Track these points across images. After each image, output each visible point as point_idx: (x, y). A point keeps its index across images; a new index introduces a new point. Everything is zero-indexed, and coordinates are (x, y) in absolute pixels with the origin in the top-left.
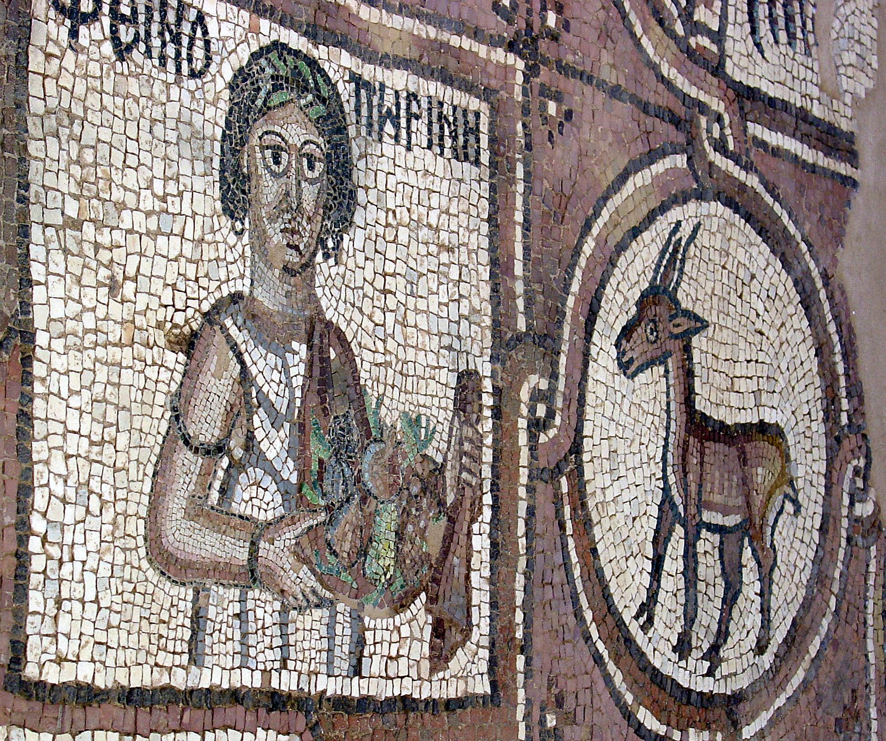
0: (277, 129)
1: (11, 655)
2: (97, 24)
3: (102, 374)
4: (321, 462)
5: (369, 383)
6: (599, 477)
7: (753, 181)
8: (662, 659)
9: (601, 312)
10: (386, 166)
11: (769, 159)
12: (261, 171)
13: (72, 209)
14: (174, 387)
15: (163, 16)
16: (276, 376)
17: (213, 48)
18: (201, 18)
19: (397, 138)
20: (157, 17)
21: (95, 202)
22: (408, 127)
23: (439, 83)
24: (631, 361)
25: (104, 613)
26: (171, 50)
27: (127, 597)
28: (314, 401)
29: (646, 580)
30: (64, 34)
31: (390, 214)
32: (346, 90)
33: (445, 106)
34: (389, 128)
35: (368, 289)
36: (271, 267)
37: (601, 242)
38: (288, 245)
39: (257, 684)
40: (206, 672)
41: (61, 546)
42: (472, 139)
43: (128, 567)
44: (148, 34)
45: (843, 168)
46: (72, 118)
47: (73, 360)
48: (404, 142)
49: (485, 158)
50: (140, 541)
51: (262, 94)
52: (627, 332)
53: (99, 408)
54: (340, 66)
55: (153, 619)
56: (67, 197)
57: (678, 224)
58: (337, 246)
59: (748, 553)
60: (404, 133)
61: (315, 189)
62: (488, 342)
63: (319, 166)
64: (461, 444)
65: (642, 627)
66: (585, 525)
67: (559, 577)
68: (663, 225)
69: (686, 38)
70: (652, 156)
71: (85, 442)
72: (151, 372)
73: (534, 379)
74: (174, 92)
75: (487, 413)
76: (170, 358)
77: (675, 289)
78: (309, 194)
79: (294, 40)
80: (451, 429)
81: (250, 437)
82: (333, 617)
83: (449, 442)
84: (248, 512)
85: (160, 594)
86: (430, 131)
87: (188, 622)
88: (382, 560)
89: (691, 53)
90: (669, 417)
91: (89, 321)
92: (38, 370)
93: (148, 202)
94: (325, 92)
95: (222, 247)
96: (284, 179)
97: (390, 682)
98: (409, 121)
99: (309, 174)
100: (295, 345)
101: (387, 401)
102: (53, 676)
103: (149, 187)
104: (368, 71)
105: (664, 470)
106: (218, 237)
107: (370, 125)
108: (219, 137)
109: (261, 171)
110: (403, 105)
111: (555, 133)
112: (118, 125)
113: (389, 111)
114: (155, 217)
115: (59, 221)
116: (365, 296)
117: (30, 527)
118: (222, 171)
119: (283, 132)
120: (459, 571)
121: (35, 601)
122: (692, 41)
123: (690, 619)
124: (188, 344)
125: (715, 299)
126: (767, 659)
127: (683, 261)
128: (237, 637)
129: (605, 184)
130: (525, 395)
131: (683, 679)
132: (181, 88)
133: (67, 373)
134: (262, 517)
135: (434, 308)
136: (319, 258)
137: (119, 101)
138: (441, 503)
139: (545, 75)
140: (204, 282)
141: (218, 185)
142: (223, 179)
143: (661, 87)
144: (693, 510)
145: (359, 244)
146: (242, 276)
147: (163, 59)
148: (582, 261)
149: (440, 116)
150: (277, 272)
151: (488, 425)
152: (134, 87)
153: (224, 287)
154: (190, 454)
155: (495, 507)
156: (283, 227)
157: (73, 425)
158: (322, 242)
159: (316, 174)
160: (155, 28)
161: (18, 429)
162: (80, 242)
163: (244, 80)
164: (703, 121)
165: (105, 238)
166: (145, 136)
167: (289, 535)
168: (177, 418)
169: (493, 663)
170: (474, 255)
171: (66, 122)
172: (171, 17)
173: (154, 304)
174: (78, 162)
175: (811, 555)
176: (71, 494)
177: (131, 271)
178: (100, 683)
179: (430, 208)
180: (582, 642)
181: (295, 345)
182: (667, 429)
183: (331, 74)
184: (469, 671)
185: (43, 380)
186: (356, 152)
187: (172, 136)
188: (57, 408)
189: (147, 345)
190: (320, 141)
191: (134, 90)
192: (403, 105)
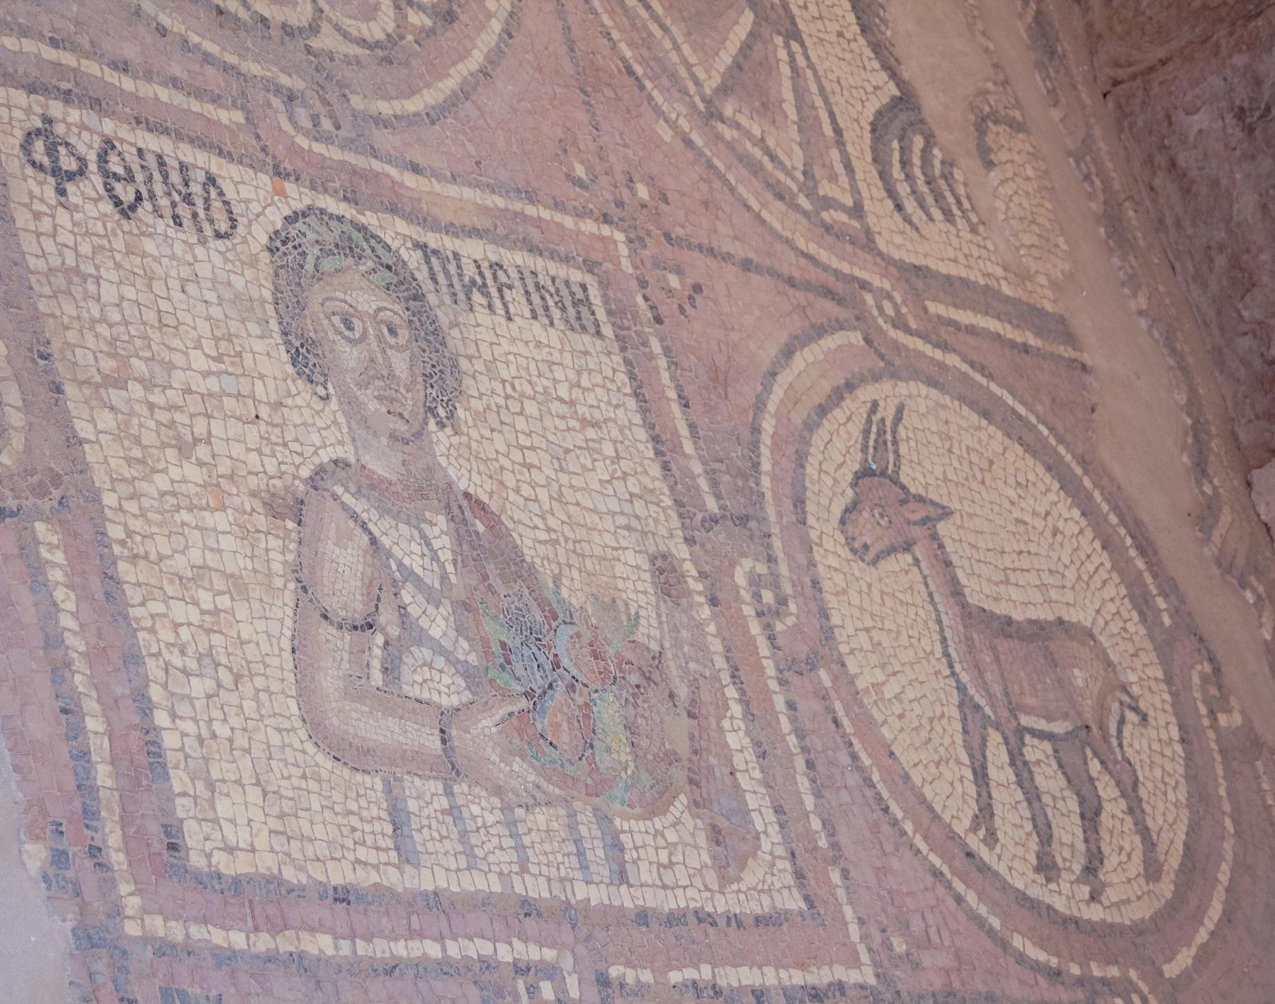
0: (341, 296)
4: (503, 645)
5: (537, 561)
7: (953, 360)
8: (1023, 878)
12: (331, 336)
15: (166, 177)
18: (211, 180)
19: (490, 307)
23: (525, 254)
27: (295, 781)
29: (972, 790)
30: (50, 193)
31: (507, 385)
32: (413, 259)
33: (540, 276)
34: (477, 297)
38: (389, 412)
40: (426, 873)
42: (584, 311)
45: (1067, 352)
46: (85, 278)
54: (397, 234)
56: (99, 355)
58: (451, 416)
59: (1095, 766)
65: (984, 841)
66: (867, 725)
67: (853, 779)
70: (820, 331)
73: (747, 564)
77: (896, 472)
78: (400, 364)
80: (659, 615)
87: (384, 815)
88: (616, 753)
89: (828, 228)
94: (387, 259)
96: (363, 345)
97: (669, 892)
103: (198, 346)
108: (270, 299)
109: (331, 336)
111: (687, 307)
113: (473, 282)
117: (150, 700)
119: (347, 298)
120: (721, 771)
122: (824, 215)
123: (1044, 833)
126: (1166, 888)
130: (740, 578)
131: (1060, 904)
132: (208, 249)
136: (432, 425)
140: (295, 446)
143: (803, 261)
150: (384, 441)
153: (321, 452)
155: (745, 702)
156: (376, 393)
161: (107, 593)
164: (869, 299)
167: (487, 723)
170: (627, 432)
172: (175, 177)
175: (1181, 770)
182: (939, 622)
185: (122, 543)
190: (397, 307)
192: (488, 274)
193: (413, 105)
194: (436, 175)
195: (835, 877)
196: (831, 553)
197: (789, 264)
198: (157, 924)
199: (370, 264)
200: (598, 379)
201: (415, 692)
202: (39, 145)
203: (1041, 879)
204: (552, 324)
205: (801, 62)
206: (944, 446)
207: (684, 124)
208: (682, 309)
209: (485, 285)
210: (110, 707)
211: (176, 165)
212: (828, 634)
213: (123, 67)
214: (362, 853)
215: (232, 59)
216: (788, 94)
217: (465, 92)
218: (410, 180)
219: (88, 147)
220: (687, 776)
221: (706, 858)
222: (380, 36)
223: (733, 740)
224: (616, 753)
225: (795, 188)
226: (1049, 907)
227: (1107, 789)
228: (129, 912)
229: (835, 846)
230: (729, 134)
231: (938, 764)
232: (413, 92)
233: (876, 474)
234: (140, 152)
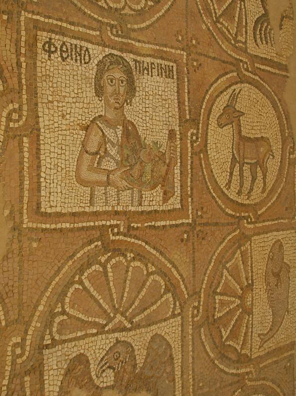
0: (112, 74)
1: (37, 206)
2: (56, 54)
3: (60, 137)
5: (142, 134)
6: (213, 153)
7: (257, 78)
9: (212, 113)
10: (145, 81)
11: (262, 73)
13: (50, 98)
14: (82, 139)
15: (76, 50)
16: (113, 135)
17: (91, 56)
18: (87, 49)
20: (74, 50)
21: (57, 96)
22: (152, 71)
24: (222, 124)
25: (64, 195)
26: (78, 58)
28: (125, 140)
29: (228, 177)
30: (47, 57)
34: (146, 72)
35: (141, 112)
36: (111, 108)
39: (110, 209)
40: (95, 207)
41: (50, 180)
42: (171, 73)
43: (70, 184)
44: (71, 54)
45: (284, 73)
47: (52, 135)
48: (150, 75)
49: (175, 77)
50: (74, 177)
51: (107, 66)
53: (60, 146)
55: (78, 195)
57: (235, 89)
58: (131, 101)
59: (259, 169)
60: (150, 73)
61: (124, 88)
62: (178, 122)
63: (125, 83)
64: (170, 147)
65: (227, 189)
66: (208, 165)
68: (230, 91)
69: (235, 44)
71: (57, 154)
72: (76, 136)
73: (192, 130)
74: (80, 68)
75: (178, 139)
76: (81, 132)
78: (122, 90)
81: (106, 149)
82: (133, 192)
83: (167, 147)
84: (106, 168)
85: (80, 190)
86: (158, 72)
87: (89, 196)
90: (234, 137)
91: (56, 125)
92: (41, 138)
93: (73, 95)
94: (126, 64)
95: (96, 104)
98: (152, 70)
99: (122, 85)
100: (118, 127)
101: (147, 139)
102: (49, 211)
104: (139, 58)
105: (232, 150)
106: (95, 102)
107: (140, 71)
110: (150, 66)
111: (196, 70)
112: (63, 77)
113: (146, 68)
114: (75, 99)
115: (47, 101)
116: (139, 113)
118: (95, 85)
121: (43, 193)
122: (237, 45)
123: (241, 186)
124: (86, 128)
125: (247, 108)
126: (265, 195)
127: (237, 99)
128: (104, 198)
129: (212, 82)
131: (240, 201)
133: (50, 138)
134: (110, 169)
135: (161, 115)
136: (125, 105)
137: (64, 71)
138: (165, 162)
139: (193, 55)
140: (90, 113)
141: (94, 89)
142: (95, 88)
143: (228, 56)
144: (242, 160)
145: (137, 101)
146: (102, 111)
147: (76, 60)
148: (206, 101)
149: (161, 68)
151: (179, 142)
152: (68, 67)
154: (88, 155)
155: (181, 162)
157: (52, 150)
158: (126, 101)
159: (124, 84)
160: (73, 53)
161: (36, 153)
162: (53, 106)
163: (101, 63)
164: (241, 64)
165: (60, 105)
166: (71, 79)
167: (119, 173)
168: (84, 147)
169: (181, 200)
171: (48, 77)
172: (78, 50)
173: (76, 119)
174: (52, 87)
175: (278, 168)
176: (52, 167)
177: (68, 112)
178: (63, 212)
179: (159, 90)
180: (208, 194)
181: (118, 127)
182: (233, 140)
183: (127, 60)
184: (175, 203)
185: (43, 140)
186: (136, 78)
187: (80, 78)
189: (74, 130)
191: (68, 68)
192: (150, 66)
194: (144, 42)
195: (190, 200)
197: (225, 58)
199: (121, 66)
200: (170, 89)
201: (104, 167)
202: (47, 45)
203: (237, 196)
204: (162, 77)
205: (243, 7)
207: (209, 24)
208: (195, 70)
209: (149, 69)
210: (30, 179)
211: (79, 47)
212: (206, 146)
214: (81, 205)
215: (100, 19)
216: (237, 15)
218: (137, 44)
221: (161, 198)
222: (140, 8)
223: (176, 171)
225: (232, 38)
226: (237, 202)
228: (25, 222)
229: (191, 193)
230: (219, 26)
231: (222, 173)
232: (144, 22)
233: (229, 107)
234: (71, 45)
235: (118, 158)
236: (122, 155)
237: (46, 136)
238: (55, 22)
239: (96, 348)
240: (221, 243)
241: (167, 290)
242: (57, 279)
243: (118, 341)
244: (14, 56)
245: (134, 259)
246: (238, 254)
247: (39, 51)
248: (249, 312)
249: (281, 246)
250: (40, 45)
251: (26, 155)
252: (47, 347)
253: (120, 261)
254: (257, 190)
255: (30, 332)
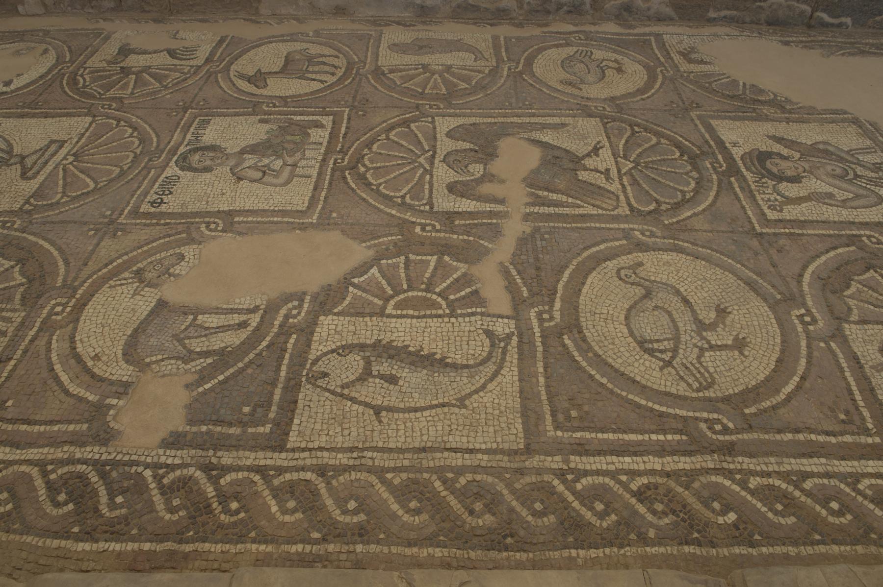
7: (227, 59)
8: (335, 79)
13: (204, 203)
32: (189, 147)
37: (235, 92)
45: (229, 38)
52: (256, 86)
66: (300, 96)
68: (234, 79)
70: (217, 81)
78: (211, 154)
79: (175, 158)
88: (297, 138)
89: (194, 73)
102: (306, 205)
104: (185, 143)
123: (327, 72)
124: (240, 179)
126: (341, 56)
130: (266, 109)
131: (341, 74)
152: (179, 191)
184: (327, 121)
188: (248, 205)
193: (155, 140)
194: (171, 139)
196: (265, 92)
198: (315, 217)
206: (247, 65)
210: (273, 216)
213: (139, 187)
217: (154, 130)
218: (172, 144)
219: (155, 197)
220: (304, 129)
224: (297, 138)
227: (321, 59)
232: (152, 139)
233: (249, 80)
235: (272, 158)
236: (272, 155)
237: (237, 206)
238: (134, 199)
239: (443, 174)
240: (376, 88)
241: (409, 127)
242: (371, 201)
243: (444, 161)
244: (158, 227)
245: (370, 149)
246: (391, 76)
247: (158, 210)
248: (448, 68)
249: (394, 45)
250: (153, 210)
251: (250, 219)
252: (432, 208)
253: (369, 158)
254: (336, 62)
255: (414, 220)
